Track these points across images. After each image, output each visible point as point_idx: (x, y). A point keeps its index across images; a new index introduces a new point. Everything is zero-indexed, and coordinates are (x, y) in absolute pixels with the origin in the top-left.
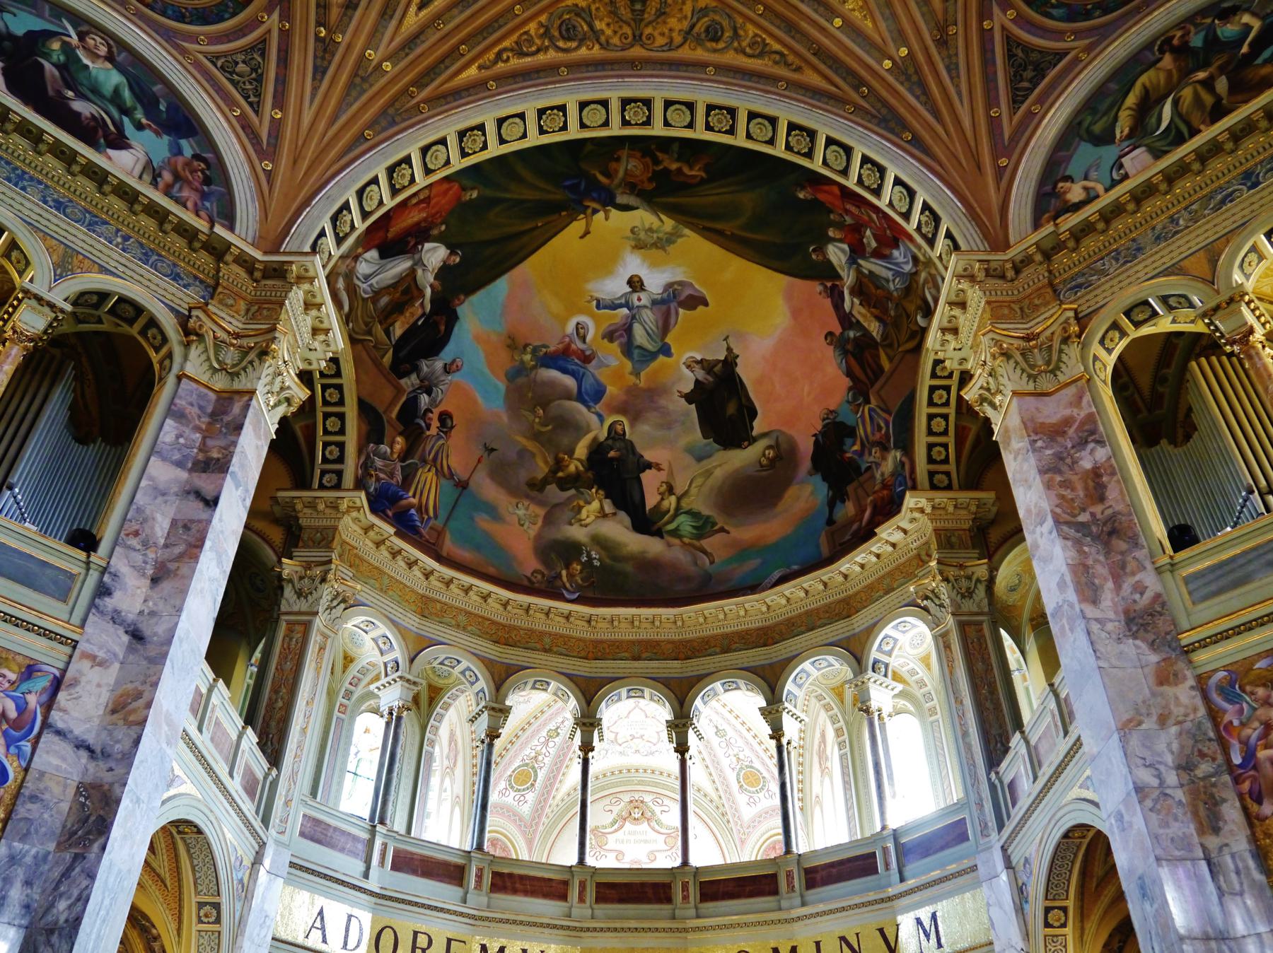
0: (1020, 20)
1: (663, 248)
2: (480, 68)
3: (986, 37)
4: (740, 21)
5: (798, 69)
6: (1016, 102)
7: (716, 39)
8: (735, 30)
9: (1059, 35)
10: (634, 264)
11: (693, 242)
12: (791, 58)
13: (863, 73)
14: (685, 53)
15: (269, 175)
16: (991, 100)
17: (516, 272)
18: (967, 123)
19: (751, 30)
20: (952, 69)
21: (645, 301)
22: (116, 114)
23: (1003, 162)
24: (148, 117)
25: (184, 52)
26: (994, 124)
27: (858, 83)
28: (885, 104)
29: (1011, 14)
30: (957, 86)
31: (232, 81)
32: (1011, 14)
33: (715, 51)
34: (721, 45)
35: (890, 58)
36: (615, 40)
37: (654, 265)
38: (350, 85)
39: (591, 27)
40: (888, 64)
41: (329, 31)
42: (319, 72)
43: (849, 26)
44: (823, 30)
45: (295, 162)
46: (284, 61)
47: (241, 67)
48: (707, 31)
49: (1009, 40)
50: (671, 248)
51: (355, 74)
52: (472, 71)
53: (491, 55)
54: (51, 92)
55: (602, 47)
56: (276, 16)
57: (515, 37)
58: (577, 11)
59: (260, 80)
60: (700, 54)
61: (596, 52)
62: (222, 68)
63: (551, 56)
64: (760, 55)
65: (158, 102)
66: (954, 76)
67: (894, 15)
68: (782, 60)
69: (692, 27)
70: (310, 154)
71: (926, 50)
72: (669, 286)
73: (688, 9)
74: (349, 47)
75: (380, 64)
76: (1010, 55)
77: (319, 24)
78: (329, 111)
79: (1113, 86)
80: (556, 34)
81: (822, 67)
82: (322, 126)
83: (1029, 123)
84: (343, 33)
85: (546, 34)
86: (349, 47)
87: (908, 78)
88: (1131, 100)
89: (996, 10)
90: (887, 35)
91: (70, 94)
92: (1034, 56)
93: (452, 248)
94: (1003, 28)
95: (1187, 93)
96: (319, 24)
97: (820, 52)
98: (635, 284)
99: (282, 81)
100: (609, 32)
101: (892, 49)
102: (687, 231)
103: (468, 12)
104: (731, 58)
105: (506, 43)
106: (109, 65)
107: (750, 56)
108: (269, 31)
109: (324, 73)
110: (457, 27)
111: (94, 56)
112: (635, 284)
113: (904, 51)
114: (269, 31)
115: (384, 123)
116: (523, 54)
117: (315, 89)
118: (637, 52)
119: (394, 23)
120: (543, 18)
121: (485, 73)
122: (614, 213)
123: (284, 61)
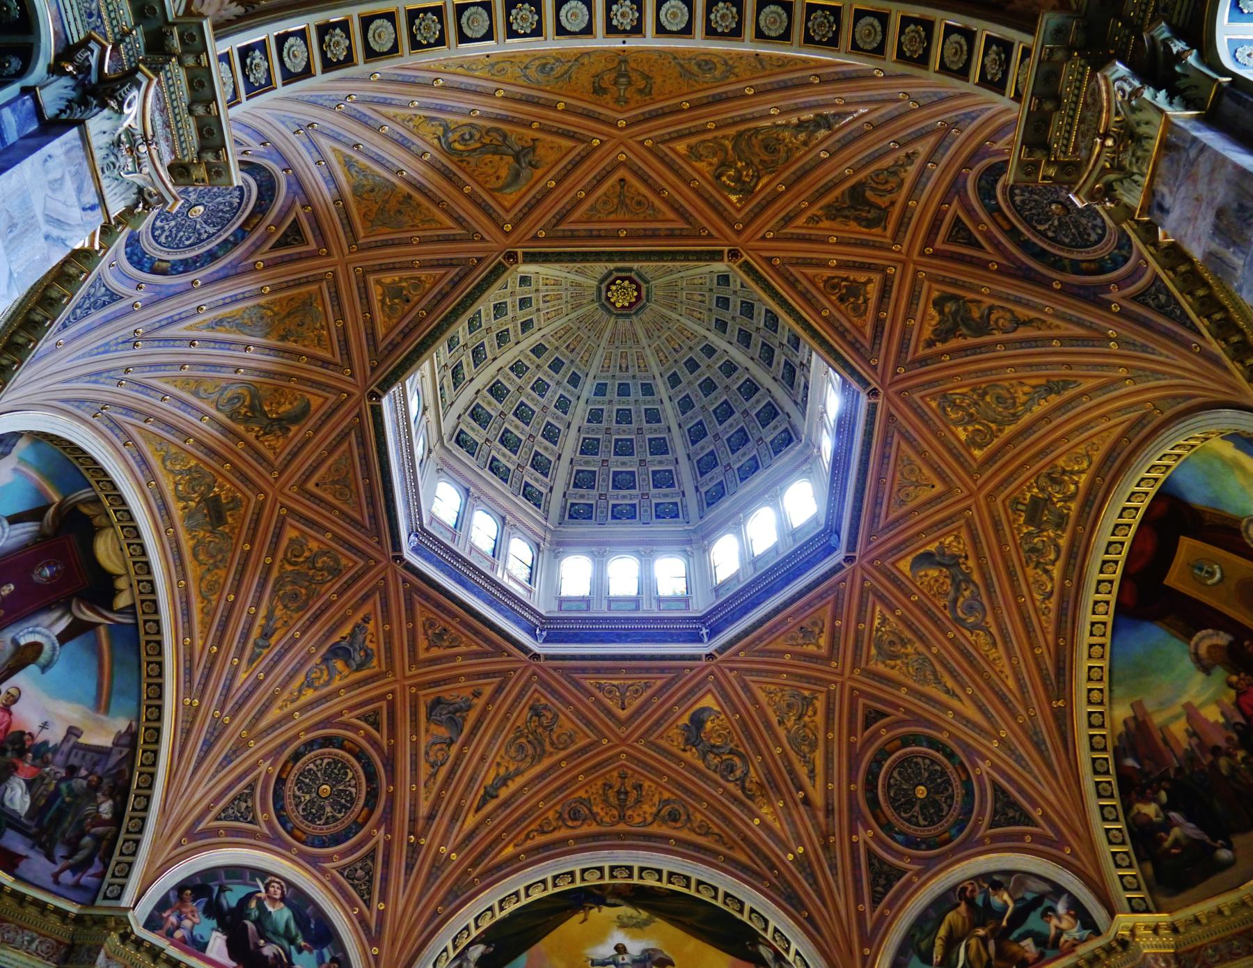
0: (876, 838)
1: (640, 927)
2: (516, 845)
3: (854, 847)
4: (691, 810)
5: (731, 848)
6: (875, 902)
7: (675, 820)
8: (688, 816)
9: (900, 856)
10: (619, 937)
11: (661, 925)
12: (726, 839)
13: (774, 859)
14: (655, 829)
15: (376, 957)
16: (859, 899)
17: (533, 949)
18: (843, 913)
19: (699, 817)
20: (833, 867)
21: (627, 959)
22: (286, 944)
23: (867, 951)
24: (305, 940)
25: (324, 872)
26: (861, 916)
27: (772, 867)
28: (790, 885)
29: (870, 833)
30: (836, 882)
31: (352, 885)
32: (870, 833)
33: (675, 828)
34: (679, 825)
35: (792, 853)
36: (607, 819)
37: (633, 937)
38: (430, 874)
39: (590, 810)
40: (791, 857)
41: (418, 838)
42: (410, 867)
43: (764, 824)
44: (747, 825)
45: (393, 944)
46: (387, 864)
47: (360, 873)
48: (670, 814)
49: (870, 853)
50: (647, 928)
51: (433, 866)
52: (510, 850)
53: (522, 836)
54: (252, 947)
55: (598, 824)
56: (382, 831)
57: (538, 822)
58: (581, 801)
59: (370, 881)
60: (665, 830)
61: (594, 828)
62: (347, 878)
63: (562, 833)
64: (706, 835)
65: (310, 922)
66: (835, 875)
67: (794, 823)
68: (720, 839)
69: (659, 812)
70: (402, 934)
71: (815, 851)
72: (645, 951)
73: (656, 799)
74: (430, 846)
75: (449, 855)
76: (870, 864)
77: (410, 833)
78: (415, 898)
79: (933, 914)
80: (566, 816)
81: (748, 850)
82: (410, 909)
83: (882, 925)
84: (426, 837)
85: (560, 817)
86: (430, 846)
87: (804, 870)
88: (942, 932)
89: (860, 829)
90: (789, 834)
91: (262, 942)
92: (885, 867)
93: (488, 945)
94: (865, 842)
95: (973, 942)
96: (410, 833)
97: (745, 839)
98: (621, 949)
99: (385, 879)
100: (602, 814)
101: (793, 845)
102: (657, 919)
103: (508, 811)
104: (685, 834)
105: (532, 827)
106: (282, 905)
107: (700, 834)
108: (378, 842)
109: (412, 868)
110: (500, 823)
111: (273, 900)
112: (621, 949)
113: (801, 850)
114: (378, 842)
115: (450, 898)
116: (543, 833)
117: (406, 881)
118: (622, 827)
119: (459, 824)
120: (558, 808)
121: (519, 849)
122: (605, 909)
123: (387, 864)
